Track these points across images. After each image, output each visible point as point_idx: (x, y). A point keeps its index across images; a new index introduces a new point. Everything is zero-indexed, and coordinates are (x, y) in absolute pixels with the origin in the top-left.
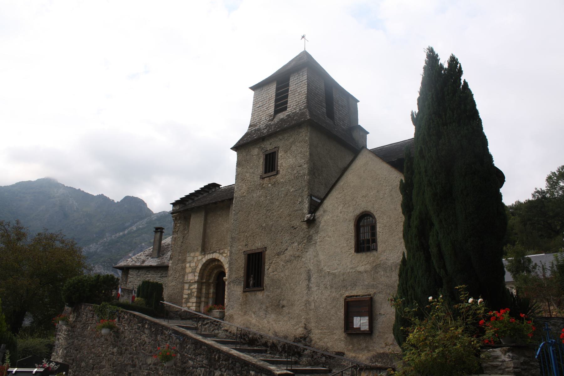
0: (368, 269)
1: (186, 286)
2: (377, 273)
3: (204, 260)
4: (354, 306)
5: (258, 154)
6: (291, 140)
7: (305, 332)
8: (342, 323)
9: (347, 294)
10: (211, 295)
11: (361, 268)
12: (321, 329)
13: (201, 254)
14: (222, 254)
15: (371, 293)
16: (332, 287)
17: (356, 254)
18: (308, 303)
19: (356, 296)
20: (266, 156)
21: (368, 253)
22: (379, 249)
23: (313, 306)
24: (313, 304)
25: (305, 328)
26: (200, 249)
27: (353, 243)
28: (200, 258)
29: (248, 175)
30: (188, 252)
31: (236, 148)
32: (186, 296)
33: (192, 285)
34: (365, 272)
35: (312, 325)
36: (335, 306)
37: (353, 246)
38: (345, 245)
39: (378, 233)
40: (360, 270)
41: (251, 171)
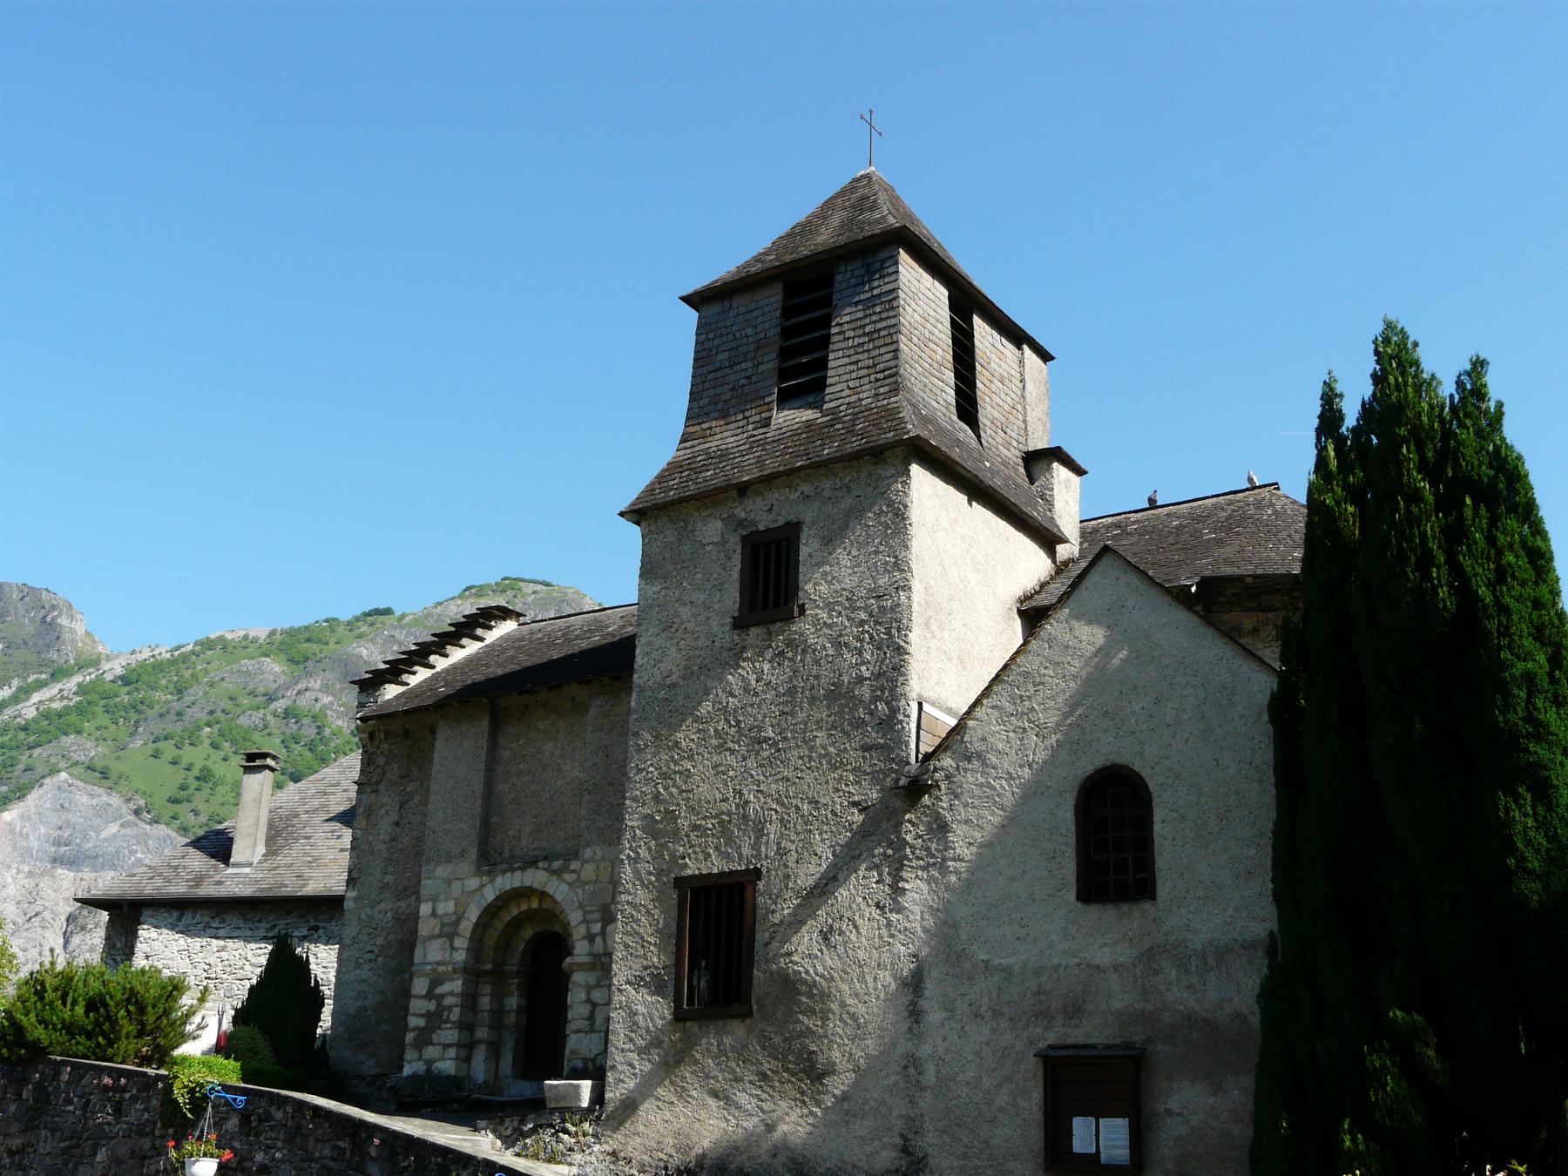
1: (420, 986)
2: (1156, 972)
3: (490, 894)
4: (1080, 1079)
5: (724, 542)
6: (847, 502)
7: (904, 1163)
8: (1036, 1136)
9: (1052, 1038)
10: (511, 1019)
11: (1103, 957)
12: (964, 1156)
13: (478, 872)
14: (558, 873)
15: (1136, 1038)
16: (997, 1014)
17: (1080, 905)
18: (912, 1064)
19: (1084, 1047)
21: (1125, 907)
22: (1163, 891)
24: (931, 1069)
25: (905, 1150)
26: (473, 853)
27: (1070, 867)
28: (473, 883)
29: (685, 612)
30: (428, 861)
31: (636, 514)
32: (421, 1022)
33: (441, 983)
34: (1116, 969)
35: (930, 1140)
36: (1008, 1079)
37: (1072, 879)
38: (1044, 873)
39: (1157, 840)
40: (1097, 961)
41: (699, 597)
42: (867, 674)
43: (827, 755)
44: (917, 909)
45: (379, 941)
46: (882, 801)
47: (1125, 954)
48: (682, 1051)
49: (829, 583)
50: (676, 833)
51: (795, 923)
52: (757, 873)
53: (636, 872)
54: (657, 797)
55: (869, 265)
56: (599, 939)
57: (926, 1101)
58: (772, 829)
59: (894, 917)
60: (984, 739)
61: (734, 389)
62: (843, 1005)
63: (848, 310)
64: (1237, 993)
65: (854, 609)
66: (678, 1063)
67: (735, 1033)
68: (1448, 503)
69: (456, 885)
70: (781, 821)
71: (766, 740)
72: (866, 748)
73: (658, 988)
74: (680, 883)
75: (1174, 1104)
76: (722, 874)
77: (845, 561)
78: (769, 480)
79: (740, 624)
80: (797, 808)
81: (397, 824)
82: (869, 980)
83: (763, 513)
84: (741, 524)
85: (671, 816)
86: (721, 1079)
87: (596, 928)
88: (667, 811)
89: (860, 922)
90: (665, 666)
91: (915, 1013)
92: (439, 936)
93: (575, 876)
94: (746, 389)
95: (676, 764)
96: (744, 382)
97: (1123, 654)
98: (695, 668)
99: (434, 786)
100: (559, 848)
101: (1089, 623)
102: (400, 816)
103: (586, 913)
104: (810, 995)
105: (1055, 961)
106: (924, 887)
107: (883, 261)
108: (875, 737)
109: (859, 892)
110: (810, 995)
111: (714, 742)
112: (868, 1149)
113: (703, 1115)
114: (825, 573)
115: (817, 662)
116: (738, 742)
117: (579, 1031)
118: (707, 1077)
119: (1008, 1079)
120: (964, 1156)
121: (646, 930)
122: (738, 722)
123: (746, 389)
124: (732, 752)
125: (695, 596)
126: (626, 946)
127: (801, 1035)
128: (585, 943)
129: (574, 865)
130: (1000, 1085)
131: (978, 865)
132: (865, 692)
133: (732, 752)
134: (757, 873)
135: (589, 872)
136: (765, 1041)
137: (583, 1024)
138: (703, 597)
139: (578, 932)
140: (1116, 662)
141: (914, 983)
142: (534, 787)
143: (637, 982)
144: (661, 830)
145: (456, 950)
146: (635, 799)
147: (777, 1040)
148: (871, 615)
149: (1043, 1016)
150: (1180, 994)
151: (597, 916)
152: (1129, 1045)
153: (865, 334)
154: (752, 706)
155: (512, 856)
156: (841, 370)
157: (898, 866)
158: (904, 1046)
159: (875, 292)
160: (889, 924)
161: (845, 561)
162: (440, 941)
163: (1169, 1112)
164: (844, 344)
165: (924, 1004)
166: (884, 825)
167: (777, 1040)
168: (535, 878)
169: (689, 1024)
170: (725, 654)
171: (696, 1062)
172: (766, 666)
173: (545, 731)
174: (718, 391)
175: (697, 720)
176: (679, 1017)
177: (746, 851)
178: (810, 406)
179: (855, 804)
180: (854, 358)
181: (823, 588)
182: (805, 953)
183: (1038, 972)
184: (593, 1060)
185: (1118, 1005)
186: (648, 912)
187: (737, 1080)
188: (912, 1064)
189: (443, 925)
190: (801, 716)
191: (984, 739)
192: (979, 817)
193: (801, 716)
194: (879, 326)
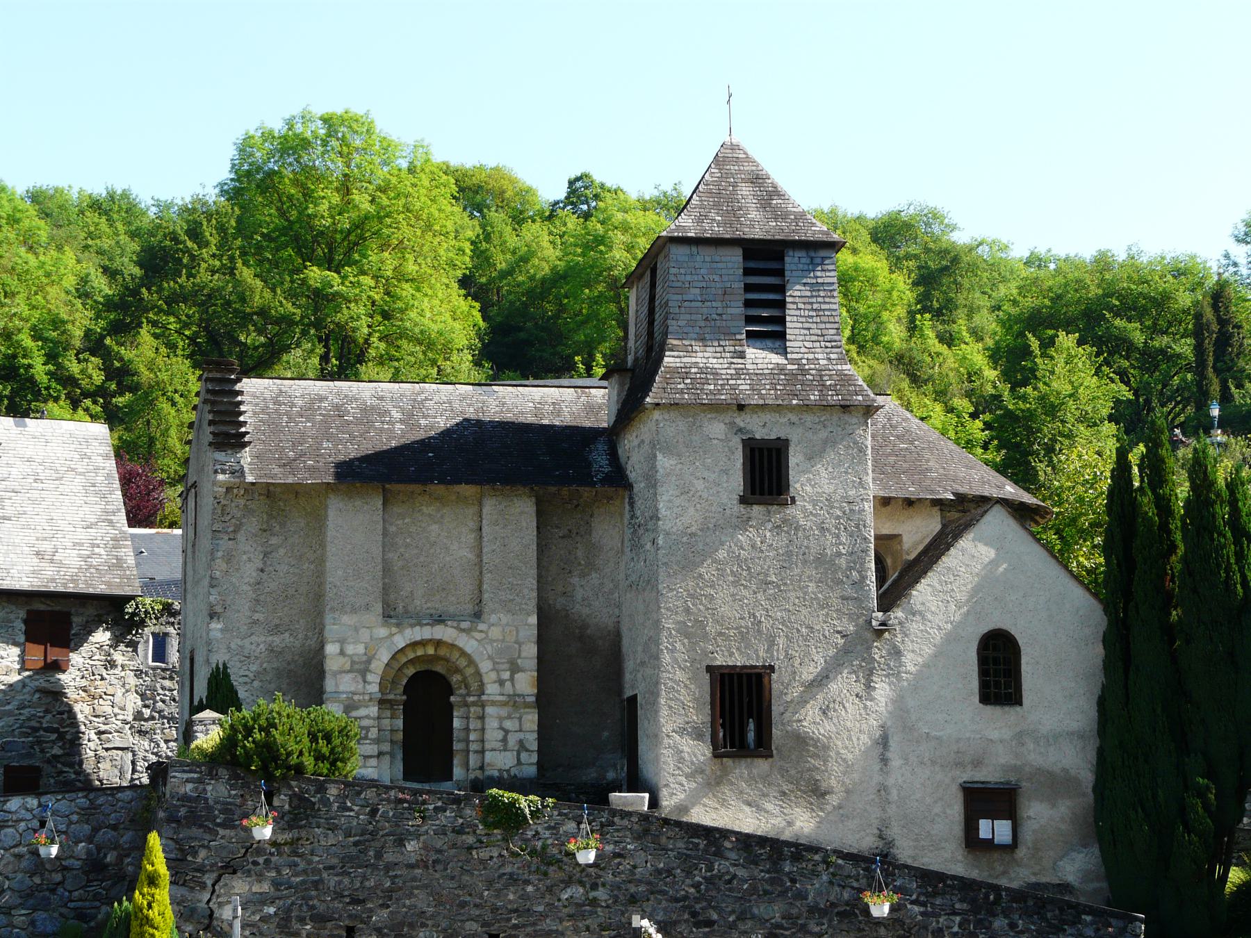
0: (1005, 737)
3: (400, 642)
4: (987, 800)
5: (727, 440)
6: (823, 434)
7: (881, 844)
8: (958, 829)
9: (966, 777)
11: (995, 735)
12: (916, 840)
13: (386, 624)
14: (467, 631)
16: (933, 763)
18: (882, 789)
20: (752, 450)
21: (1007, 708)
23: (894, 795)
24: (894, 792)
26: (378, 607)
27: (975, 684)
28: (383, 632)
29: (699, 485)
30: (332, 609)
33: (357, 708)
35: (895, 832)
36: (941, 799)
37: (977, 691)
38: (960, 686)
42: (844, 551)
43: (817, 598)
44: (883, 700)
45: (254, 668)
46: (856, 632)
47: (1007, 734)
48: (721, 776)
49: (813, 486)
50: (705, 636)
51: (803, 702)
52: (772, 668)
53: (675, 660)
54: (687, 610)
55: (812, 258)
56: (508, 684)
57: (892, 810)
58: (781, 641)
59: (868, 703)
60: (923, 604)
61: (706, 319)
62: (838, 753)
63: (798, 287)
64: (1076, 760)
65: (832, 507)
66: (718, 784)
67: (762, 765)
68: (1237, 542)
69: (365, 635)
70: (787, 636)
71: (771, 583)
72: (844, 598)
73: (699, 736)
74: (710, 669)
75: (1031, 813)
76: (744, 667)
77: (824, 474)
78: (763, 407)
79: (743, 500)
80: (798, 631)
81: (262, 571)
82: (855, 739)
83: (763, 428)
84: (740, 430)
85: (700, 624)
86: (752, 794)
87: (506, 675)
88: (696, 621)
89: (847, 705)
90: (686, 520)
91: (884, 761)
92: (349, 672)
93: (483, 635)
94: (718, 323)
95: (701, 589)
96: (715, 316)
97: (1005, 566)
98: (711, 526)
99: (331, 549)
100: (452, 609)
101: (986, 544)
102: (265, 563)
103: (495, 663)
104: (816, 746)
105: (967, 735)
106: (887, 687)
107: (823, 258)
108: (850, 592)
109: (843, 685)
110: (816, 746)
111: (731, 578)
112: (857, 836)
113: (741, 816)
114: (809, 480)
115: (807, 538)
116: (750, 581)
117: (493, 750)
118: (741, 792)
119: (941, 799)
120: (916, 840)
121: (684, 696)
122: (749, 568)
123: (718, 323)
124: (745, 587)
125: (706, 474)
126: (670, 707)
127: (809, 770)
128: (497, 685)
129: (481, 627)
130: (936, 802)
131: (919, 676)
132: (843, 562)
133: (745, 587)
134: (772, 668)
135: (495, 633)
136: (783, 772)
137: (499, 745)
138: (713, 476)
139: (489, 677)
140: (1001, 569)
142: (422, 559)
143: (681, 731)
144: (693, 632)
145: (369, 683)
146: (668, 609)
147: (793, 772)
148: (844, 513)
149: (959, 764)
150: (1037, 757)
151: (506, 666)
152: (1008, 783)
153: (812, 309)
154: (759, 558)
155: (406, 612)
156: (797, 332)
157: (870, 673)
158: (877, 778)
159: (820, 280)
160: (865, 707)
161: (824, 474)
162: (351, 675)
163: (1029, 818)
164: (797, 313)
165: (889, 755)
166: (859, 647)
167: (793, 772)
168: (444, 633)
169: (725, 760)
170: (734, 520)
171: (732, 784)
172: (768, 534)
173: (430, 515)
174: (694, 317)
175: (714, 561)
176: (716, 755)
177: (761, 654)
178: (772, 350)
179: (838, 632)
180: (806, 325)
181: (808, 489)
182: (810, 720)
183: (958, 740)
184: (508, 771)
185: (1002, 761)
186: (686, 686)
187: (765, 795)
188: (882, 789)
189: (353, 663)
190: (797, 571)
191: (923, 604)
192: (921, 649)
193: (797, 571)
194: (823, 307)
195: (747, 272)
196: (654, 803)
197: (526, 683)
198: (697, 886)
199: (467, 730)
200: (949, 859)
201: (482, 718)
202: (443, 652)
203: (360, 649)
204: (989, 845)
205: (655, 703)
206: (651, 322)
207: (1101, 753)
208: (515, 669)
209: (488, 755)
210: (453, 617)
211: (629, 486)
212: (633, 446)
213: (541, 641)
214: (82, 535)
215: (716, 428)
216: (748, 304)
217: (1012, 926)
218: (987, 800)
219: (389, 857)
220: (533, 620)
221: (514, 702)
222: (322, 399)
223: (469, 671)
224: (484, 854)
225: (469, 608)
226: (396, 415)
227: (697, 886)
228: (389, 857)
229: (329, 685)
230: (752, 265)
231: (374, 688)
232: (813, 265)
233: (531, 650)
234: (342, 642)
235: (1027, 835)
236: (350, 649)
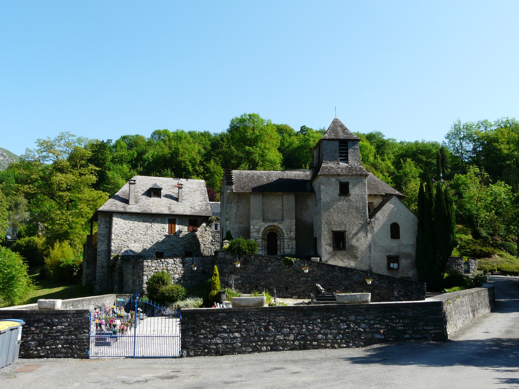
4: (392, 259)
6: (356, 181)
8: (386, 266)
11: (394, 245)
14: (280, 223)
18: (370, 257)
23: (372, 258)
28: (262, 224)
29: (330, 192)
35: (372, 266)
41: (332, 190)
47: (397, 245)
51: (352, 238)
54: (327, 219)
57: (372, 261)
58: (348, 225)
64: (411, 250)
67: (344, 252)
68: (447, 203)
69: (259, 224)
73: (330, 245)
74: (332, 231)
79: (339, 195)
83: (343, 180)
85: (330, 222)
86: (341, 258)
91: (370, 251)
99: (251, 206)
100: (277, 219)
108: (362, 215)
109: (361, 235)
121: (327, 237)
135: (286, 224)
139: (285, 233)
141: (370, 247)
143: (326, 245)
144: (329, 224)
149: (386, 252)
150: (403, 250)
157: (367, 232)
158: (369, 255)
168: (276, 224)
176: (334, 250)
182: (354, 242)
188: (370, 257)
195: (340, 146)
196: (321, 260)
197: (293, 234)
198: (330, 277)
199: (280, 244)
200: (384, 272)
201: (284, 242)
202: (275, 228)
203: (258, 227)
204: (393, 269)
205: (320, 239)
206: (319, 157)
207: (417, 249)
208: (290, 231)
209: (285, 250)
210: (277, 220)
211: (315, 192)
212: (315, 183)
213: (296, 225)
214: (200, 203)
215: (333, 180)
216: (340, 153)
217: (398, 286)
218: (392, 259)
219: (264, 271)
220: (294, 221)
221: (290, 238)
222: (249, 174)
223: (281, 232)
224: (284, 270)
225: (281, 219)
226: (265, 177)
227: (330, 277)
228: (264, 271)
229: (251, 235)
230: (341, 144)
231: (261, 235)
232: (354, 144)
233: (294, 227)
234: (254, 226)
235: (401, 266)
236: (256, 227)
